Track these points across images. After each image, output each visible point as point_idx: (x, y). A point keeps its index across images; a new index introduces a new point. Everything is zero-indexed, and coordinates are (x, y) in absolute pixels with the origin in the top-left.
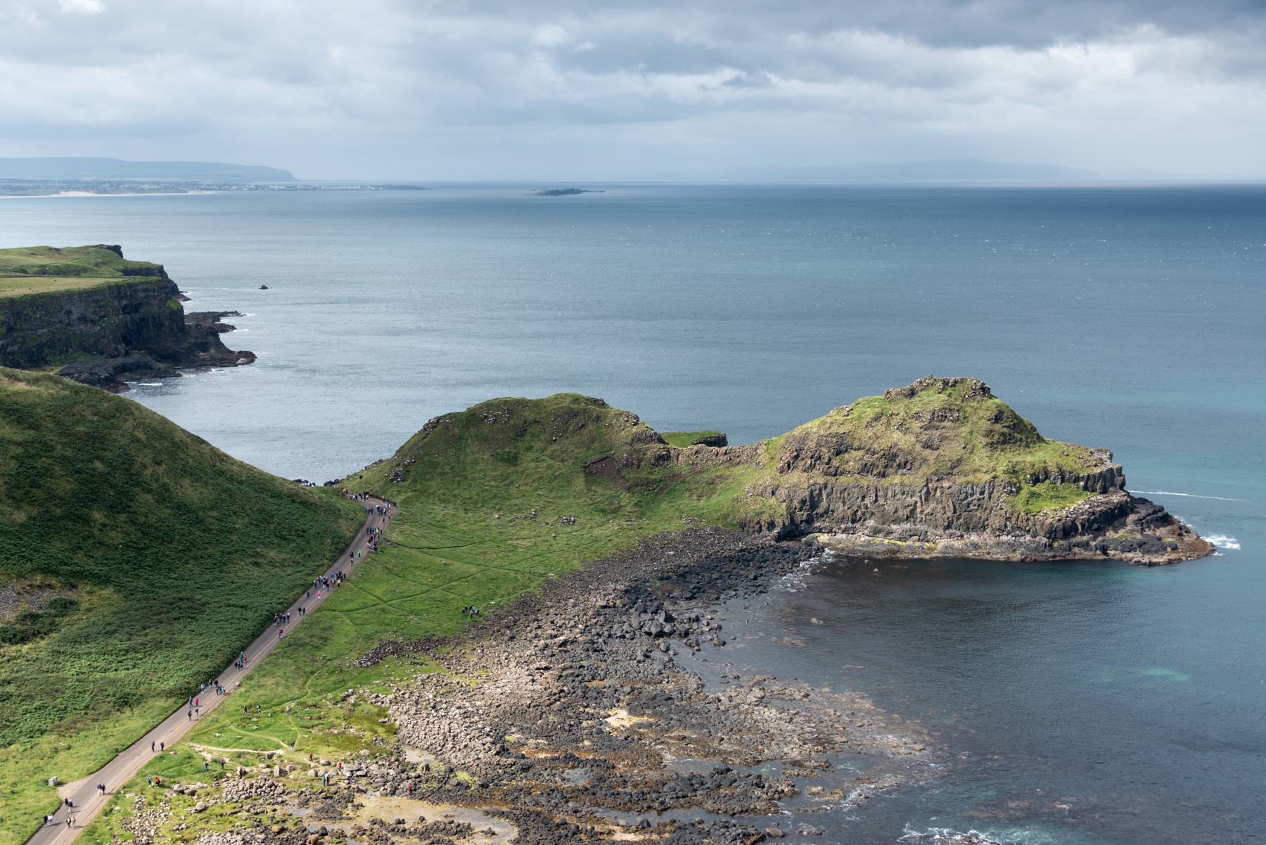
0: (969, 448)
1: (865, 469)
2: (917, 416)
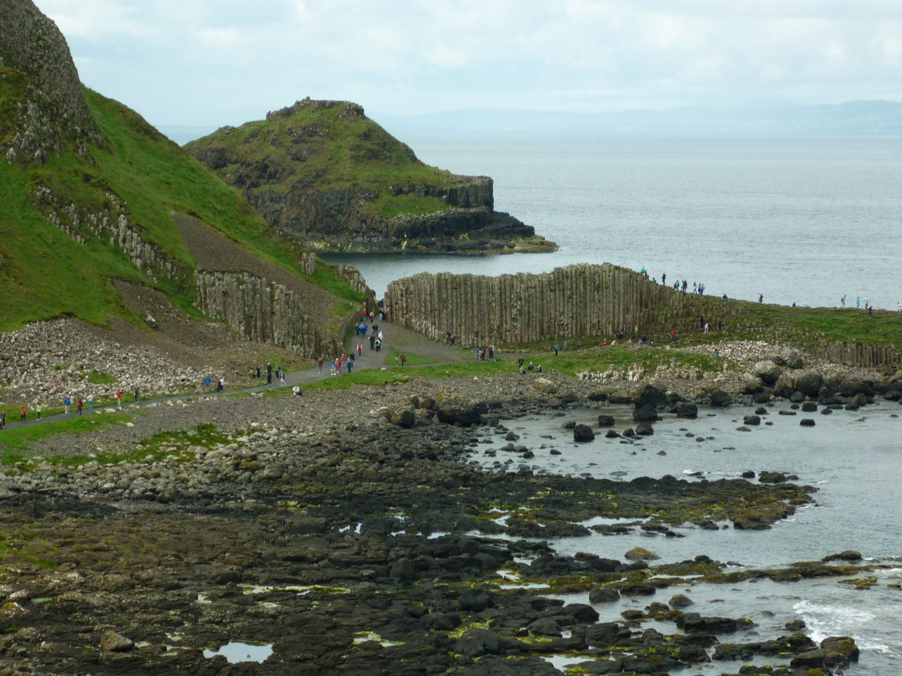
2: (290, 132)
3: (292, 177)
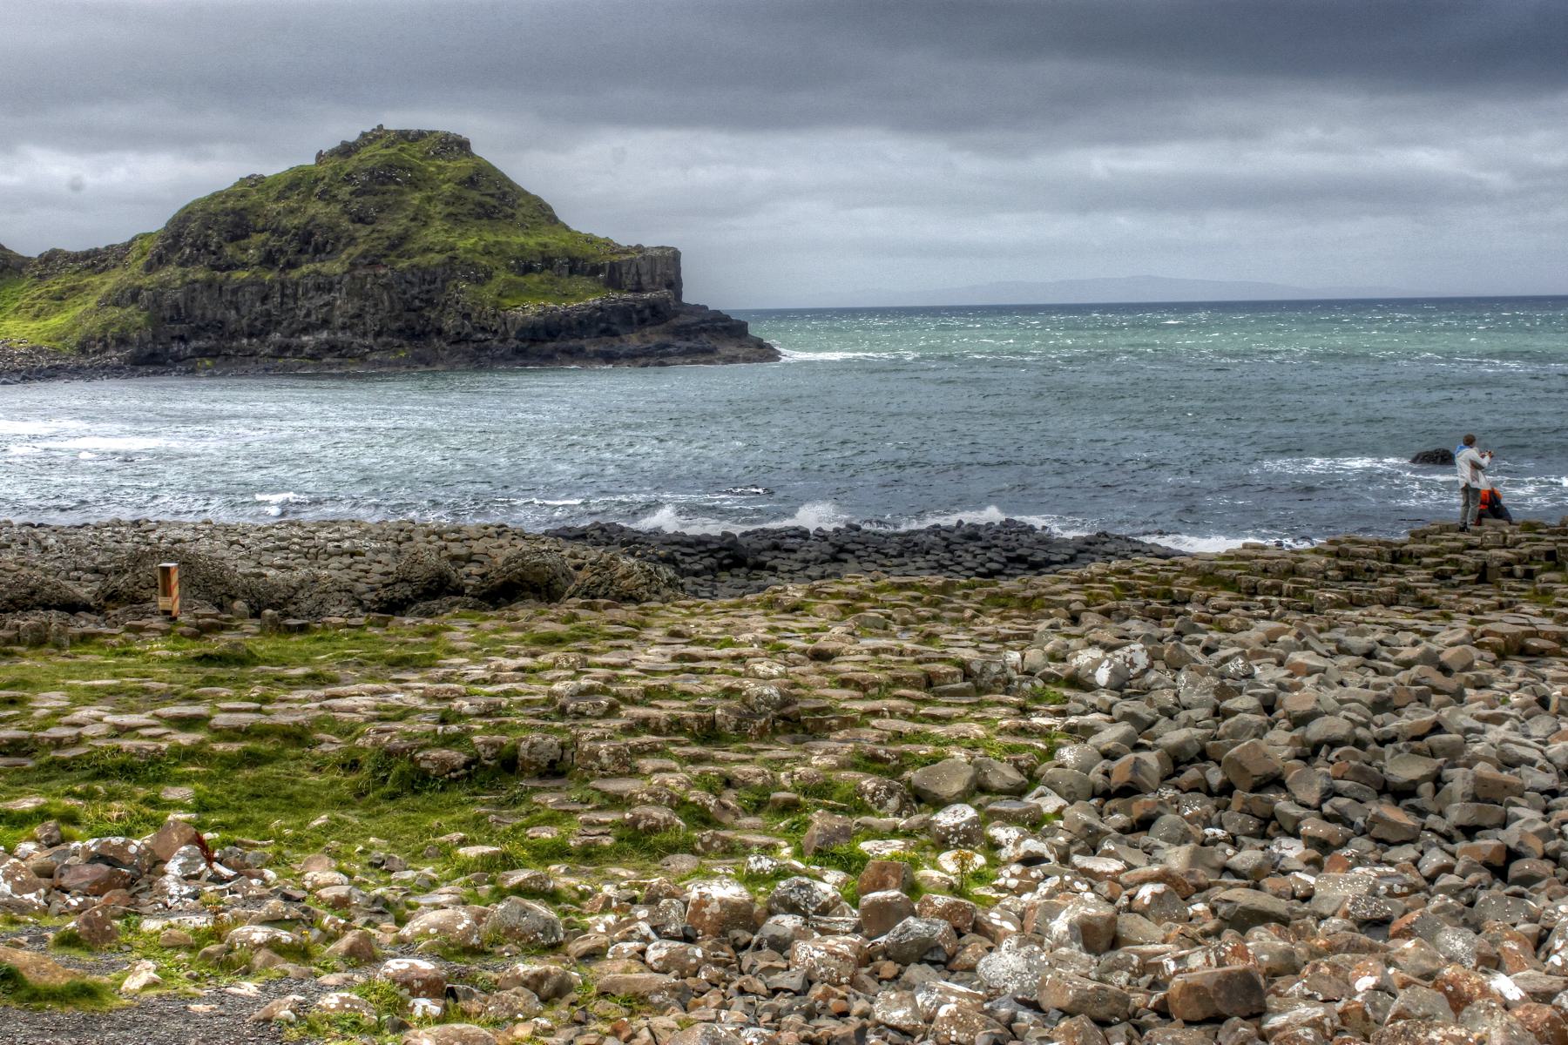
0: (421, 219)
1: (269, 260)
2: (349, 179)
3: (351, 250)
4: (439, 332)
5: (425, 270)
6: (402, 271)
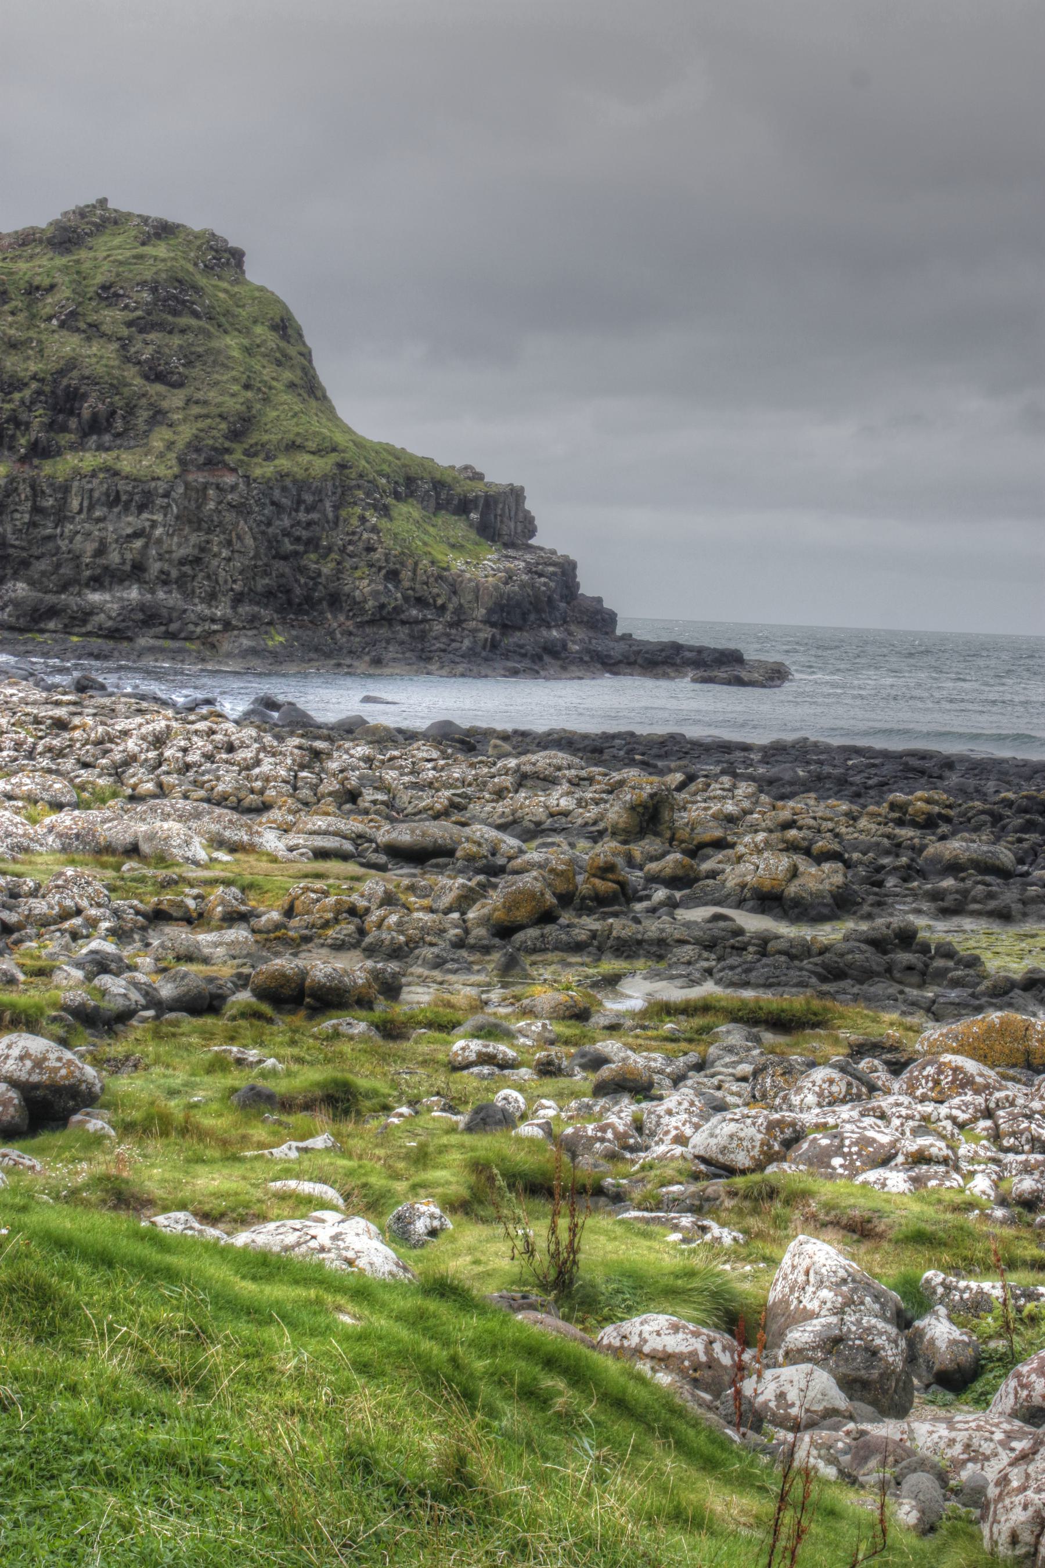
2: (108, 294)
4: (335, 600)
5: (302, 485)
6: (268, 484)
